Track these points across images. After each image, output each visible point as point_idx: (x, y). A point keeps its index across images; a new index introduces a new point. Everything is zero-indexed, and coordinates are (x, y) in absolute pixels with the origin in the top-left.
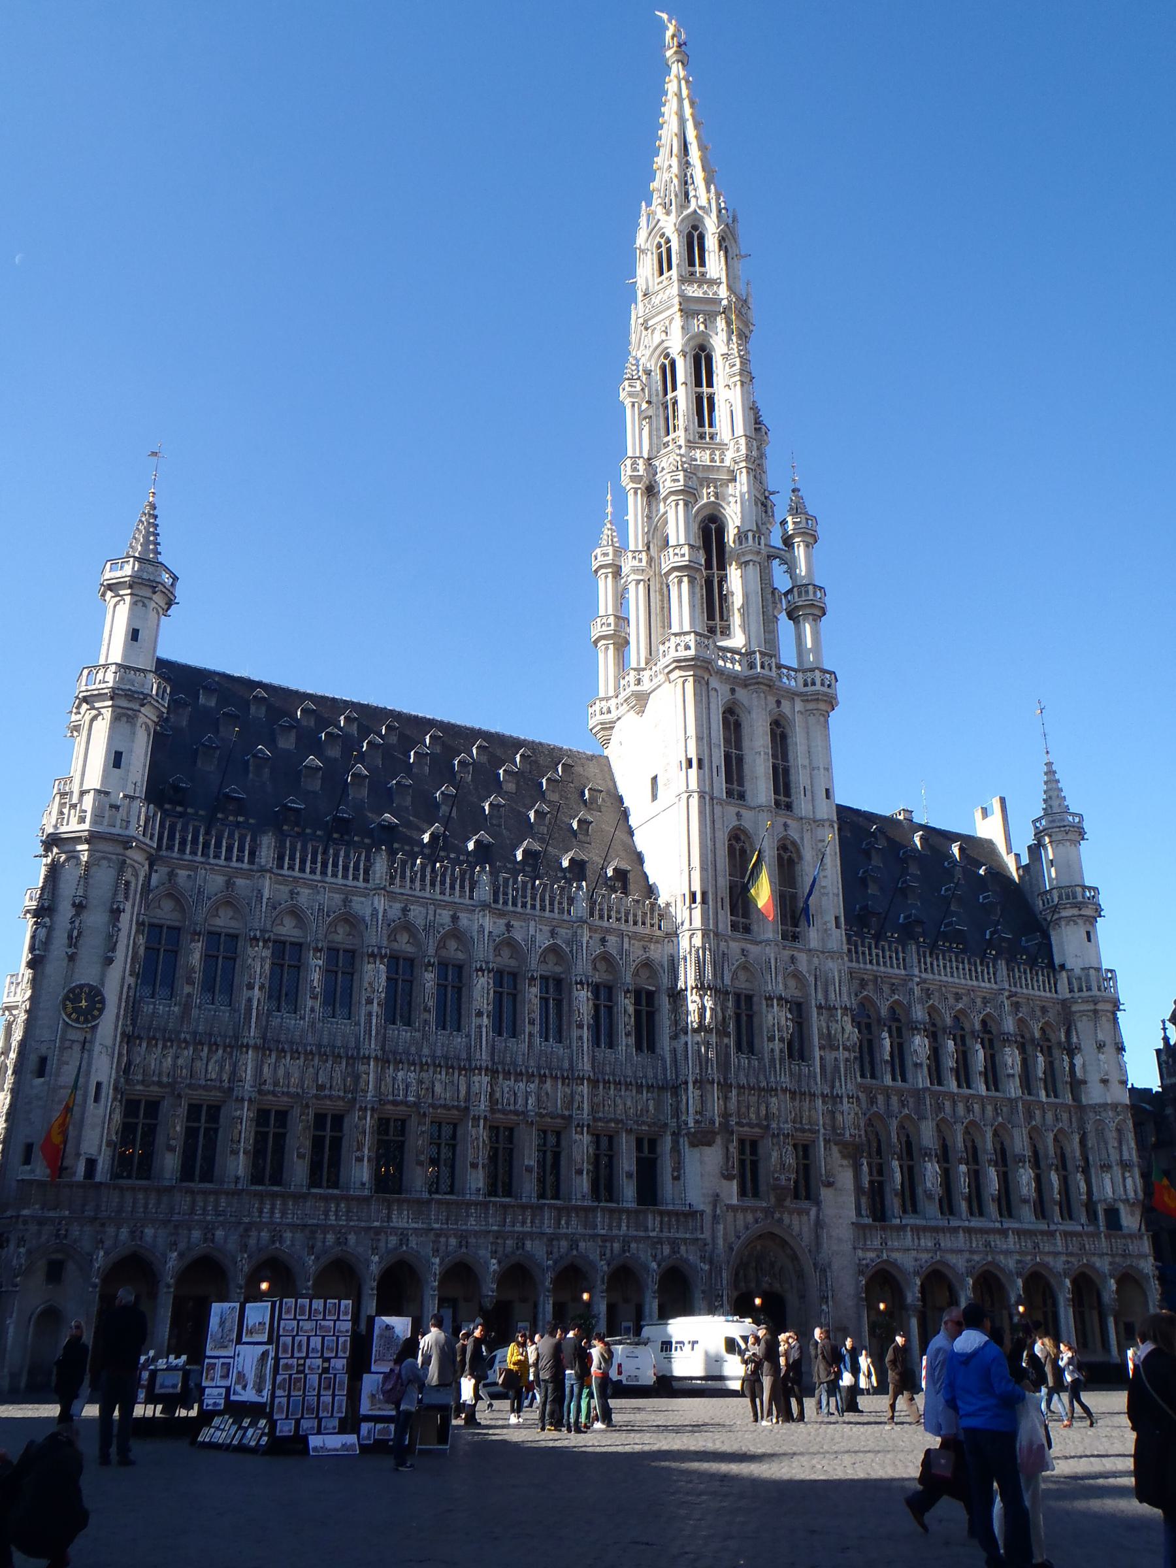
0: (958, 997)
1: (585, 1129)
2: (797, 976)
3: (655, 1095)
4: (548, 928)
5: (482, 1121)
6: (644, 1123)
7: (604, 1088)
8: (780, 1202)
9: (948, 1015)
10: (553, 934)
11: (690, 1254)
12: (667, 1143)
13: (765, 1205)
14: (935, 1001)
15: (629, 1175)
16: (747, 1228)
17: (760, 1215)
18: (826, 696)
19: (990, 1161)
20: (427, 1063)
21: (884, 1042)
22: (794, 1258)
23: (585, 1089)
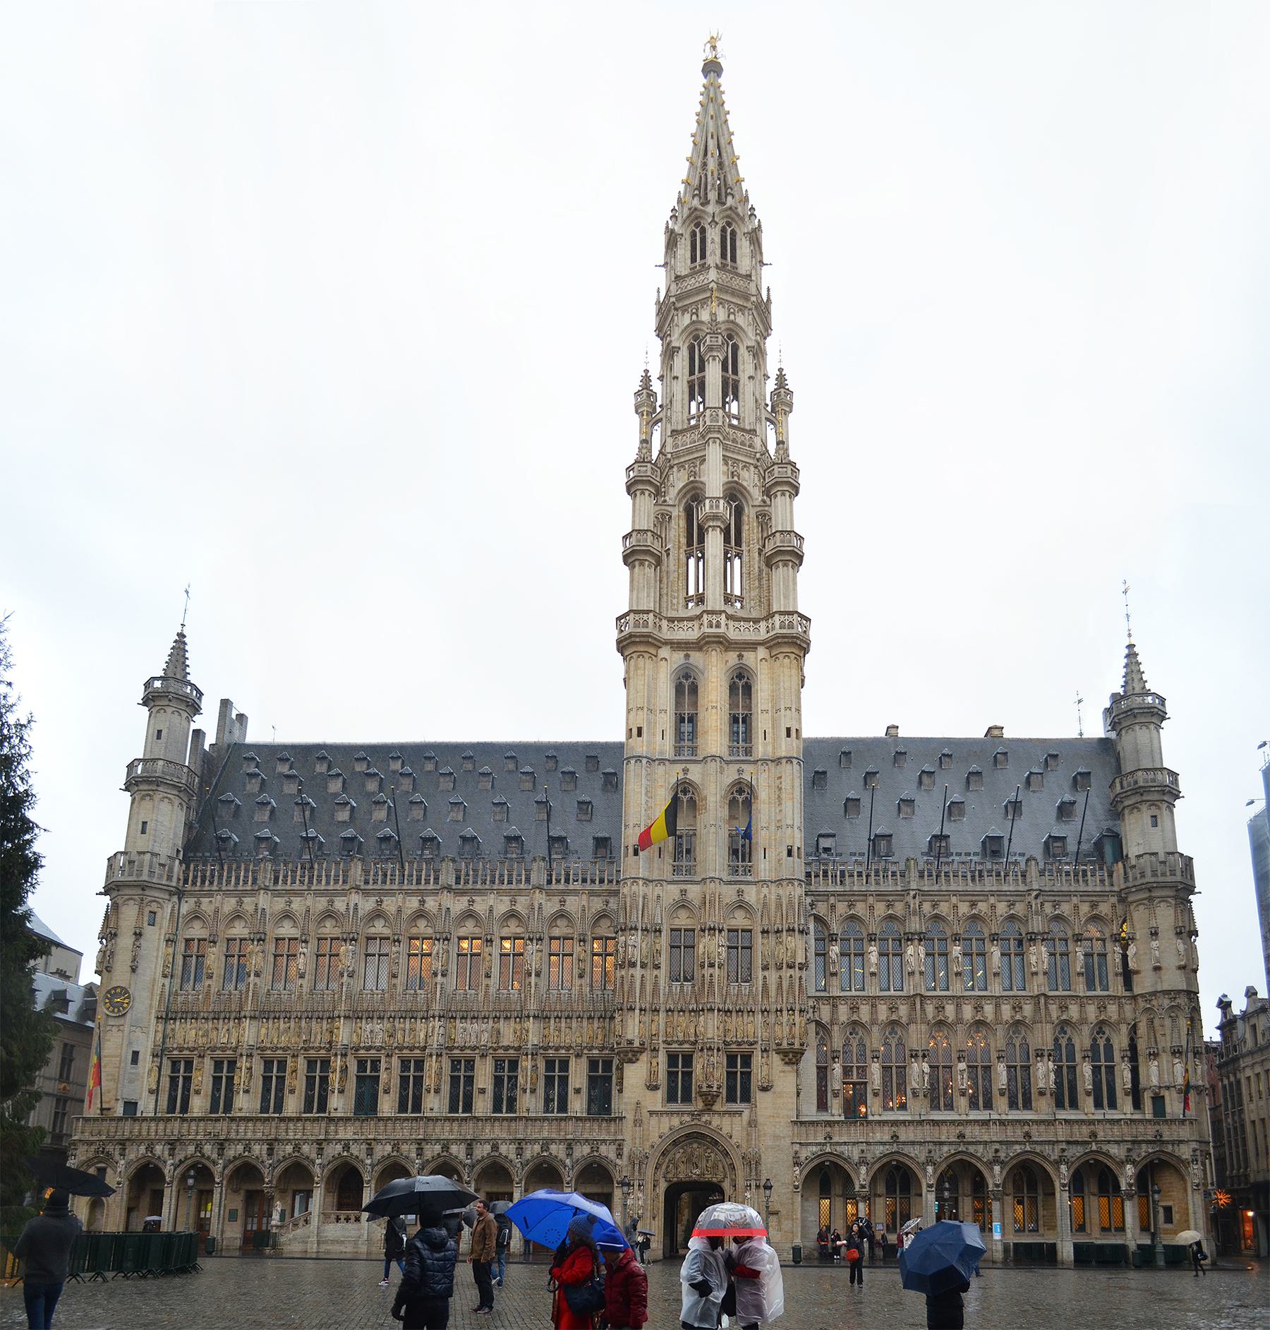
0: (973, 905)
1: (530, 1056)
2: (741, 905)
3: (607, 1025)
4: (508, 898)
10: (513, 902)
11: (608, 1151)
12: (615, 1062)
13: (691, 1108)
15: (578, 1091)
17: (687, 1118)
18: (783, 637)
21: (870, 956)
23: (531, 1024)
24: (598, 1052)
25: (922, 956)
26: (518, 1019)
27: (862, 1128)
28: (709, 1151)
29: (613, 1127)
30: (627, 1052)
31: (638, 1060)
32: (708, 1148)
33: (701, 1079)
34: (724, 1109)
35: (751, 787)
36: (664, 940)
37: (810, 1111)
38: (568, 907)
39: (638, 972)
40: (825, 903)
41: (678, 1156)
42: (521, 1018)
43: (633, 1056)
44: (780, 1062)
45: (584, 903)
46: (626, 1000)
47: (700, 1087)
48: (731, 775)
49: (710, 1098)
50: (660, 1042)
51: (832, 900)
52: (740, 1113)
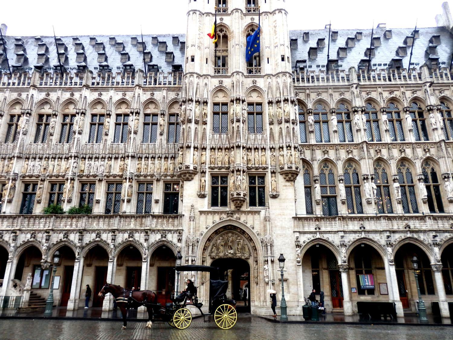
0: (391, 92)
1: (128, 180)
2: (255, 89)
4: (122, 93)
5: (69, 181)
6: (166, 176)
7: (145, 160)
8: (238, 207)
9: (382, 101)
11: (172, 238)
13: (228, 209)
14: (374, 95)
15: (157, 202)
16: (213, 223)
17: (224, 216)
19: (419, 180)
20: (46, 158)
21: (333, 121)
22: (251, 240)
23: (129, 161)
24: (170, 178)
25: (365, 120)
26: (122, 159)
27: (340, 222)
28: (239, 238)
29: (176, 222)
30: (185, 173)
31: (192, 179)
32: (239, 236)
33: (233, 189)
34: (249, 209)
35: (259, 27)
36: (209, 109)
37: (303, 213)
38: (155, 97)
39: (193, 126)
40: (304, 94)
41: (219, 241)
42: (124, 158)
43: (190, 176)
44: (283, 180)
45: (165, 95)
46: (185, 141)
47: (232, 195)
48: (248, 20)
49: (239, 202)
50: (207, 167)
51: (308, 91)
52: (258, 212)
